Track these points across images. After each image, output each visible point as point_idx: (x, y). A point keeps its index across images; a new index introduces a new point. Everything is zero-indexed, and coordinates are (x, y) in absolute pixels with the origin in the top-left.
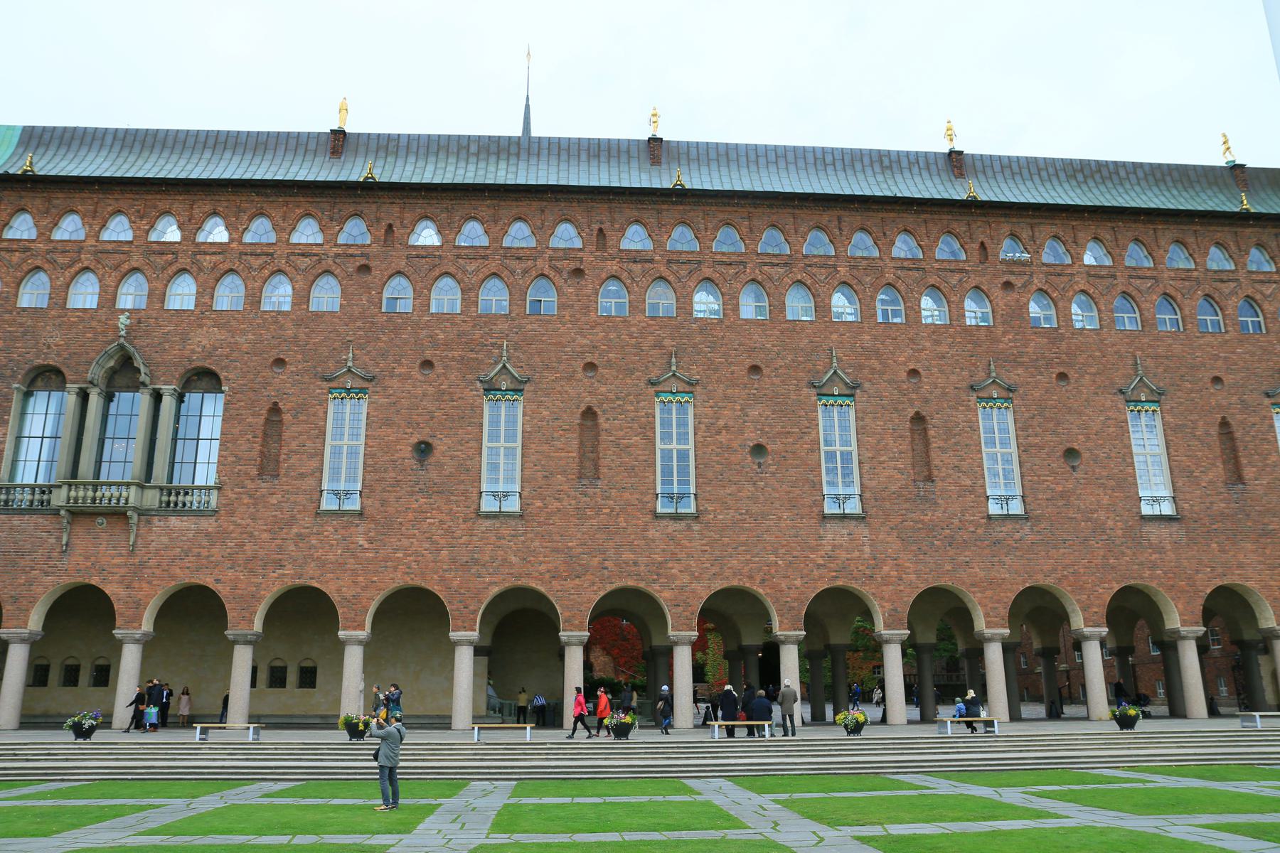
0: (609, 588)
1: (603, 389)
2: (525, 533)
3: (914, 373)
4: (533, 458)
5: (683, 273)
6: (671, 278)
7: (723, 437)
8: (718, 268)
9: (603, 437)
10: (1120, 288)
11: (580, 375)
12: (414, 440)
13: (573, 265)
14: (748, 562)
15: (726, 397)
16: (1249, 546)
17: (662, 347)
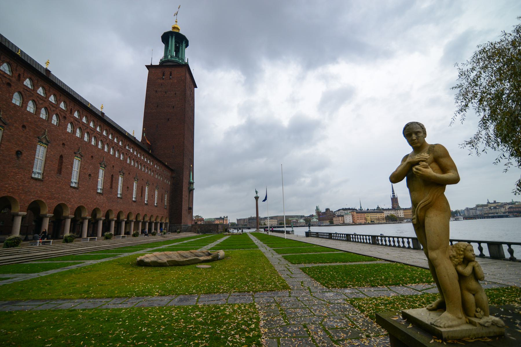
0: (59, 203)
1: (65, 151)
2: (43, 185)
3: (113, 166)
4: (48, 165)
5: (84, 128)
6: (82, 129)
7: (85, 171)
8: (90, 130)
9: (63, 164)
10: (137, 160)
11: (61, 146)
12: (17, 149)
13: (64, 115)
14: (84, 201)
15: (87, 162)
16: (141, 207)
17: (78, 145)
